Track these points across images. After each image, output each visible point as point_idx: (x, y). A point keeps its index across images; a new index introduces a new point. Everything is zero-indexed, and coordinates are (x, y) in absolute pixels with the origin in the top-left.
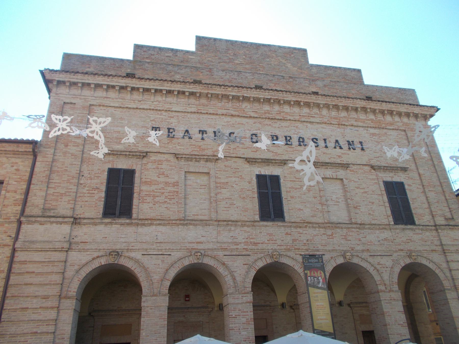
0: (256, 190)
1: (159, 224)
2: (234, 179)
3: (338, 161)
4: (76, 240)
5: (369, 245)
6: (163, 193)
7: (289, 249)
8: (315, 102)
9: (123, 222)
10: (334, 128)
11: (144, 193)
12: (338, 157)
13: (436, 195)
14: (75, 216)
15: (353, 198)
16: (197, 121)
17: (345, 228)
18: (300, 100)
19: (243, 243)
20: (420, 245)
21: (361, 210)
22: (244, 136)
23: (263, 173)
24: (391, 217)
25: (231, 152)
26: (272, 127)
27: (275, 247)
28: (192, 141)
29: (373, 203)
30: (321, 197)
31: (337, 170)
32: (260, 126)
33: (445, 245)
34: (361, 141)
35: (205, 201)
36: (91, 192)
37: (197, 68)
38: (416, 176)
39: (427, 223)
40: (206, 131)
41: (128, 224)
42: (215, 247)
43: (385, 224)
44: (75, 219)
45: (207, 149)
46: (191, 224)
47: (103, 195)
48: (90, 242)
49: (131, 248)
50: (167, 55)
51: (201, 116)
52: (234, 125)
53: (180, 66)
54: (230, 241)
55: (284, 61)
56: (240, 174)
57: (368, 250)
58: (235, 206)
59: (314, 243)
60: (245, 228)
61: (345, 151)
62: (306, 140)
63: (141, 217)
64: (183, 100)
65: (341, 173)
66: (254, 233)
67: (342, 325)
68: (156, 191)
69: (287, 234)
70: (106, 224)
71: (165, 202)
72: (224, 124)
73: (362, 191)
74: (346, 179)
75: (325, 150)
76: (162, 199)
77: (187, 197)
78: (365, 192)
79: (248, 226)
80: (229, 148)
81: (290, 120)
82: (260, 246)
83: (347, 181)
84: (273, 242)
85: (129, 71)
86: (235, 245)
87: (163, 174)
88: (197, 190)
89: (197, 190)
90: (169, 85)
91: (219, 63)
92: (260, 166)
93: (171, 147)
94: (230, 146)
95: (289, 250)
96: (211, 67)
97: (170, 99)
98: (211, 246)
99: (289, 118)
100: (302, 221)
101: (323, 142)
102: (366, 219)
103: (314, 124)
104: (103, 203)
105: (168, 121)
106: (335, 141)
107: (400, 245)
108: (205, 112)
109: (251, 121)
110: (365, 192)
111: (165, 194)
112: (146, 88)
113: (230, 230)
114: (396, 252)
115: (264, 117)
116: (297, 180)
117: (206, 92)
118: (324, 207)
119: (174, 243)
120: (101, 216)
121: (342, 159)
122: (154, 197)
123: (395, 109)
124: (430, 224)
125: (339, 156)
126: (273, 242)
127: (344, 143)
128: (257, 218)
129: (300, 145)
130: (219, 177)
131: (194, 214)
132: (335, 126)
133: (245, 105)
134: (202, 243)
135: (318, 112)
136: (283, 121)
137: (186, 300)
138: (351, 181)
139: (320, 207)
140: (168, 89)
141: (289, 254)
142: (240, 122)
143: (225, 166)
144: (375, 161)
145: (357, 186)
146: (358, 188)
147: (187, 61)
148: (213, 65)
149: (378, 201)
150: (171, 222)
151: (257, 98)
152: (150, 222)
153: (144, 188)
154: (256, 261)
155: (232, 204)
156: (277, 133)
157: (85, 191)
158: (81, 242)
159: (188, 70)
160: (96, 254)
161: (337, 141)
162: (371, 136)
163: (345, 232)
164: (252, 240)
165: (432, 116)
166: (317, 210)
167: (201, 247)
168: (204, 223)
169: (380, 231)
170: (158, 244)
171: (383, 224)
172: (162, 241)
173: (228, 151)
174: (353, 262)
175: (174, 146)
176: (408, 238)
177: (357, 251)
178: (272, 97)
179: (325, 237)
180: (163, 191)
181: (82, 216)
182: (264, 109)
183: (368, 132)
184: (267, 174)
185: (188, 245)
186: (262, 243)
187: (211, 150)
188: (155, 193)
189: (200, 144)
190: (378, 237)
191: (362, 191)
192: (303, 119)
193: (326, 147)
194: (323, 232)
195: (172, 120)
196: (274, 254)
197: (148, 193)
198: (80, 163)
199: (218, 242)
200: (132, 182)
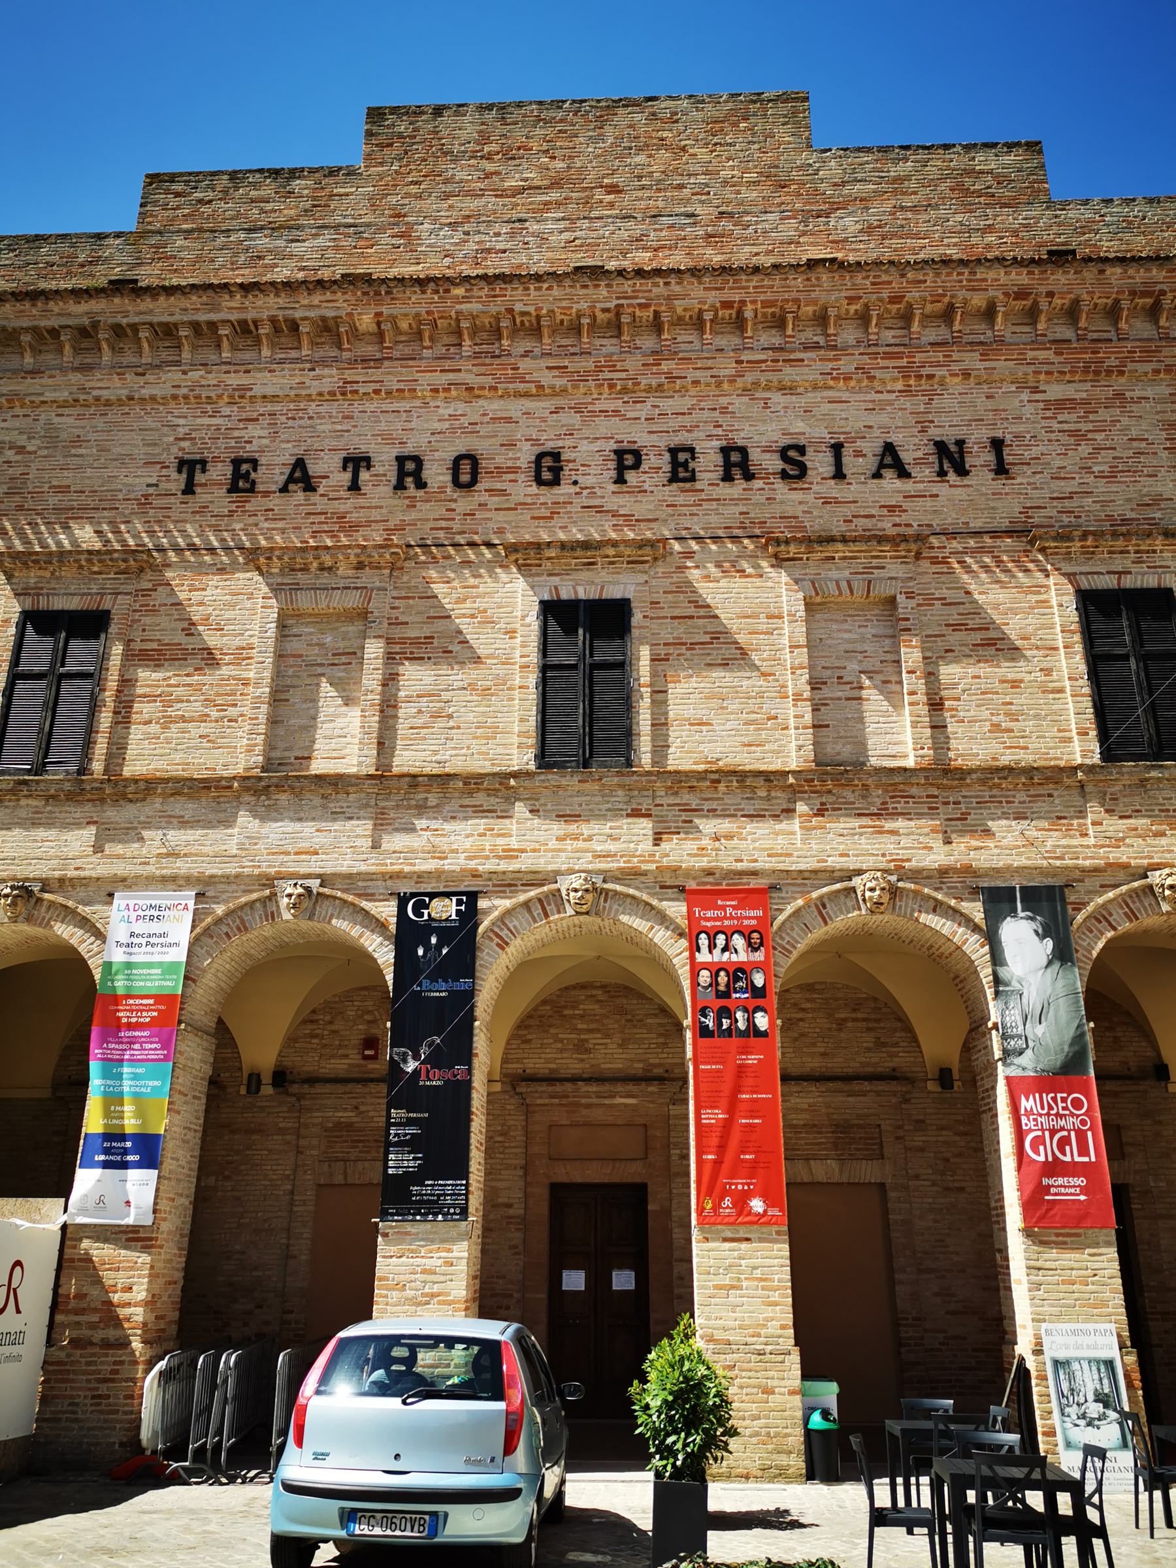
3: (887, 526)
12: (885, 512)
23: (565, 595)
25: (456, 526)
26: (624, 418)
28: (315, 498)
32: (575, 419)
34: (999, 434)
45: (369, 523)
52: (478, 428)
55: (702, 153)
61: (921, 486)
62: (755, 455)
67: (947, 1160)
71: (204, 718)
72: (438, 426)
73: (977, 637)
74: (910, 595)
75: (833, 489)
80: (449, 515)
85: (117, 272)
91: (447, 196)
94: (453, 505)
101: (828, 457)
105: (236, 434)
106: (879, 450)
112: (160, 324)
121: (904, 519)
125: (891, 509)
127: (919, 454)
129: (727, 478)
130: (402, 619)
135: (821, 340)
137: (366, 1058)
138: (929, 600)
140: (234, 317)
142: (499, 414)
144: (1054, 513)
145: (955, 619)
146: (956, 627)
156: (640, 437)
161: (889, 448)
162: (1049, 414)
163: (878, 801)
173: (443, 524)
175: (251, 520)
183: (1037, 396)
186: (534, 851)
187: (381, 526)
189: (342, 508)
191: (977, 637)
193: (839, 475)
195: (254, 431)
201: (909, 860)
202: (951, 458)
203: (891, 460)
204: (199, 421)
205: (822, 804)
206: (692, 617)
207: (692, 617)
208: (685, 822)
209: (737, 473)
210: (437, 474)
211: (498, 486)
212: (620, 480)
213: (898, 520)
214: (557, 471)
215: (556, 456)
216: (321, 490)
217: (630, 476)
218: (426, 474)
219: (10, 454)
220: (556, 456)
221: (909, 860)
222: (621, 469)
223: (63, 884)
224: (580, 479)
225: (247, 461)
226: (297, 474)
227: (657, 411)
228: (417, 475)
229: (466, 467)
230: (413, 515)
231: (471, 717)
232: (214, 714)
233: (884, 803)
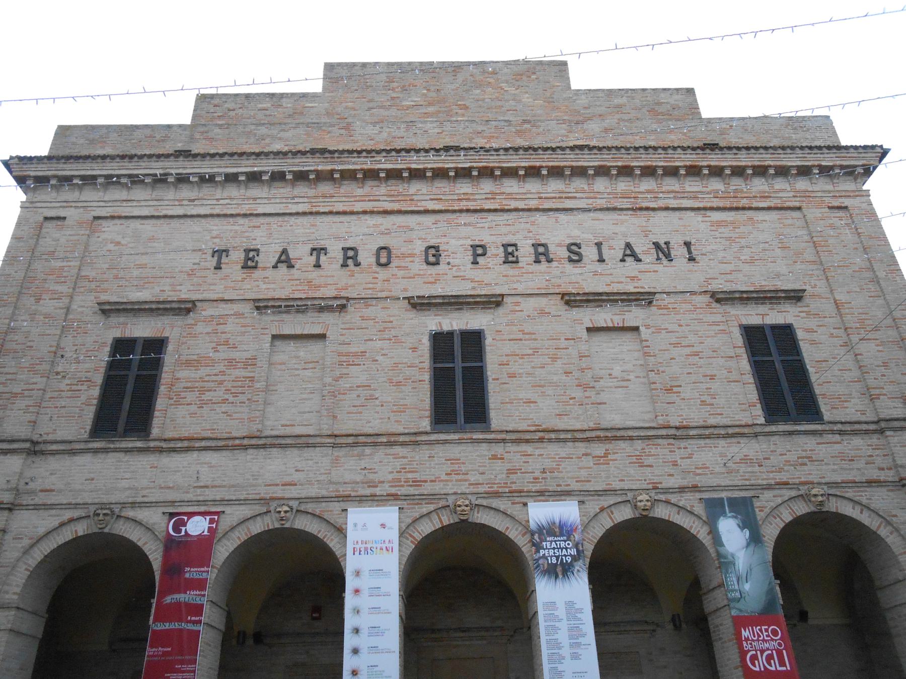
0: (427, 363)
1: (206, 449)
2: (379, 344)
4: (32, 485)
5: (699, 474)
6: (221, 383)
7: (497, 493)
8: (574, 164)
9: (130, 445)
10: (623, 217)
11: (183, 385)
13: (880, 348)
14: (35, 438)
15: (661, 369)
16: (308, 231)
17: (640, 438)
18: (538, 164)
19: (389, 482)
20: (834, 470)
21: (682, 395)
22: (410, 252)
23: (446, 328)
24: (759, 406)
27: (464, 488)
28: (294, 271)
29: (712, 377)
30: (582, 370)
31: (626, 309)
33: (901, 466)
34: (688, 239)
35: (312, 396)
36: (74, 387)
37: (318, 125)
38: (830, 308)
39: (858, 417)
40: (324, 249)
41: (141, 450)
42: (324, 493)
43: (743, 423)
44: (34, 443)
46: (273, 446)
47: (96, 392)
48: (60, 491)
49: (139, 500)
50: (260, 106)
51: (319, 219)
53: (285, 124)
54: (359, 478)
55: (512, 90)
56: (393, 332)
57: (695, 487)
58: (377, 402)
59: (561, 475)
60: (398, 450)
62: (552, 248)
63: (169, 434)
64: (282, 190)
65: (634, 316)
66: (417, 458)
68: (207, 379)
69: (494, 457)
70: (96, 451)
71: (225, 401)
72: (366, 231)
73: (688, 351)
74: (647, 327)
75: (599, 267)
76: (220, 394)
77: (272, 388)
78: (696, 354)
79: (403, 444)
81: (516, 210)
82: (427, 489)
83: (650, 331)
84: (460, 477)
85: (180, 146)
86: (369, 487)
87: (226, 343)
88: (297, 372)
89: (297, 372)
90: (250, 162)
91: (370, 109)
92: (440, 313)
93: (249, 287)
94: (376, 275)
95: (497, 495)
96: (350, 120)
97: (256, 191)
98: (313, 492)
99: (513, 204)
100: (533, 428)
101: (595, 250)
102: (695, 416)
103: (575, 213)
104: (93, 409)
105: (246, 234)
106: (623, 247)
107: (780, 470)
108: (326, 210)
109: (428, 220)
110: (696, 354)
111: (225, 383)
113: (361, 456)
114: (769, 487)
115: (457, 208)
116: (527, 337)
117: (329, 168)
118: (587, 394)
119: (233, 486)
120: (86, 436)
121: (640, 284)
122: (203, 391)
123: (772, 163)
124: (863, 418)
125: (633, 278)
126: (460, 477)
127: (645, 249)
128: (425, 424)
129: (537, 261)
131: (283, 423)
132: (625, 212)
133: (416, 188)
134: (296, 485)
135: (586, 188)
136: (501, 213)
137: (314, 619)
138: (659, 330)
139: (578, 393)
141: (495, 503)
142: (403, 224)
143: (363, 318)
144: (722, 282)
145: (674, 340)
146: (676, 345)
147: (302, 113)
148: (355, 116)
149: (725, 372)
150: (230, 443)
151: (439, 169)
152: (186, 444)
153: (183, 374)
154: (415, 520)
155: (372, 398)
156: (485, 237)
157: (63, 386)
158: (42, 491)
159: (301, 131)
160: (68, 515)
161: (628, 245)
162: (713, 228)
163: (639, 448)
164: (410, 476)
165: (868, 172)
166: (571, 402)
167: (293, 492)
168: (303, 442)
169: (729, 440)
170: (199, 491)
171: (738, 423)
172: (209, 483)
173: (371, 286)
174: (656, 515)
176: (804, 454)
177: (667, 491)
178: (475, 165)
179: (589, 462)
180: (223, 378)
181: (50, 437)
182: (457, 192)
183: (707, 219)
184: (455, 328)
185: (265, 492)
186: (432, 481)
187: (334, 287)
188: (202, 384)
189: (310, 277)
190: (722, 455)
191: (688, 351)
192: (547, 205)
193: (601, 260)
194: (583, 451)
195: (258, 233)
196: (458, 503)
197: (189, 385)
198: (58, 332)
199: (331, 482)
200: (157, 364)
201: (661, 483)
202: (663, 251)
203: (630, 253)
204: (225, 227)
205: (607, 450)
206: (521, 340)
207: (521, 340)
208: (525, 462)
209: (542, 258)
210: (366, 257)
211: (403, 264)
212: (475, 263)
213: (636, 285)
214: (437, 256)
215: (437, 248)
216: (297, 266)
217: (480, 260)
218: (360, 258)
219: (111, 247)
220: (437, 248)
221: (661, 483)
222: (476, 255)
223: (134, 505)
224: (451, 261)
225: (253, 250)
226: (283, 258)
227: (494, 223)
228: (354, 258)
229: (384, 254)
230: (351, 281)
231: (389, 399)
232: (231, 399)
233: (643, 449)
